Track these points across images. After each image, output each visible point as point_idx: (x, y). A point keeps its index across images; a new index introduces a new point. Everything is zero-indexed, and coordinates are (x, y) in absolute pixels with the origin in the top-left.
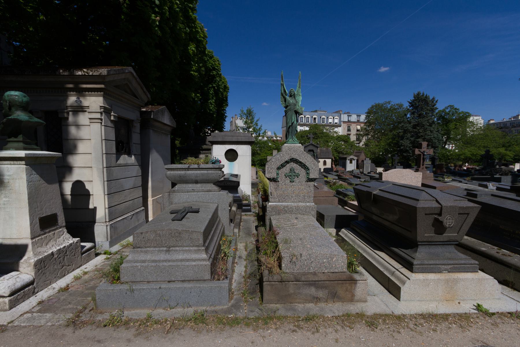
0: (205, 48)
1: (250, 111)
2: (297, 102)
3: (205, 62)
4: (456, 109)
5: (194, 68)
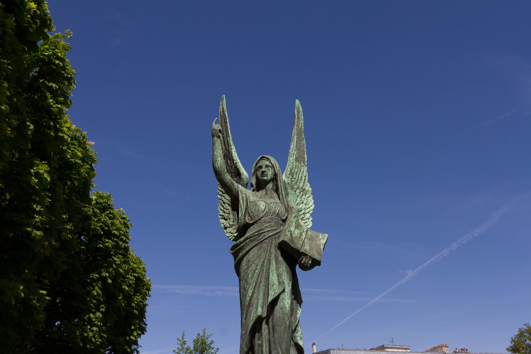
0: (86, 185)
1: (203, 343)
2: (288, 209)
3: (88, 218)
5: (38, 218)
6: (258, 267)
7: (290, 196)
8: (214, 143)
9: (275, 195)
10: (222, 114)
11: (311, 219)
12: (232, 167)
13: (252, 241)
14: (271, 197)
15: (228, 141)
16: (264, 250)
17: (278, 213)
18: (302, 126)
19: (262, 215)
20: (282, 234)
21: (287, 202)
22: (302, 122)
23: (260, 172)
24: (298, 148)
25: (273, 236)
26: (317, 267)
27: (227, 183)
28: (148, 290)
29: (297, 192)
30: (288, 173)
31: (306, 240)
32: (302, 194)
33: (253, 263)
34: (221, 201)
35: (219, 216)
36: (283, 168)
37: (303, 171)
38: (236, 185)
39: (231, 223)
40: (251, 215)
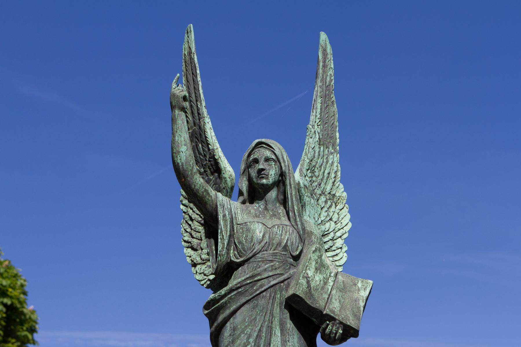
2: (304, 236)
6: (251, 340)
7: (308, 208)
8: (173, 121)
9: (281, 210)
10: (188, 58)
11: (345, 249)
12: (205, 156)
13: (240, 294)
14: (274, 215)
15: (198, 110)
16: (262, 311)
18: (331, 80)
19: (257, 247)
20: (293, 283)
21: (302, 224)
22: (331, 72)
23: (256, 171)
24: (323, 121)
25: (277, 286)
26: (351, 340)
27: (198, 190)
28: (32, 330)
29: (320, 201)
30: (306, 167)
31: (334, 292)
32: (329, 203)
33: (243, 332)
34: (186, 216)
35: (183, 243)
36: (295, 160)
37: (333, 163)
38: (213, 193)
39: (204, 256)
40: (240, 247)
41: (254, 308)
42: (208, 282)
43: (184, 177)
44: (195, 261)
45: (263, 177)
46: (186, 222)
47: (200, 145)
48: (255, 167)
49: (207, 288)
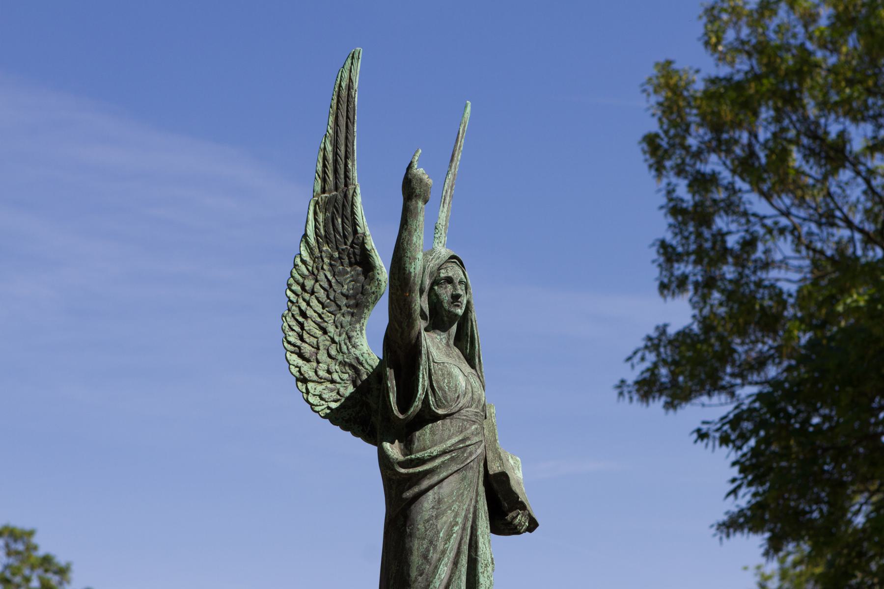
4: (46, 561)
6: (460, 520)
12: (345, 237)
17: (484, 405)
19: (463, 401)
23: (449, 294)
33: (449, 508)
40: (440, 393)
41: (462, 480)
42: (328, 411)
43: (410, 291)
44: (306, 376)
45: (458, 306)
46: (293, 315)
47: (340, 220)
48: (446, 288)
49: (326, 416)
